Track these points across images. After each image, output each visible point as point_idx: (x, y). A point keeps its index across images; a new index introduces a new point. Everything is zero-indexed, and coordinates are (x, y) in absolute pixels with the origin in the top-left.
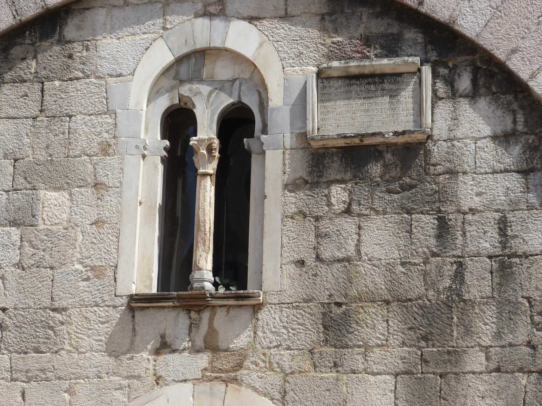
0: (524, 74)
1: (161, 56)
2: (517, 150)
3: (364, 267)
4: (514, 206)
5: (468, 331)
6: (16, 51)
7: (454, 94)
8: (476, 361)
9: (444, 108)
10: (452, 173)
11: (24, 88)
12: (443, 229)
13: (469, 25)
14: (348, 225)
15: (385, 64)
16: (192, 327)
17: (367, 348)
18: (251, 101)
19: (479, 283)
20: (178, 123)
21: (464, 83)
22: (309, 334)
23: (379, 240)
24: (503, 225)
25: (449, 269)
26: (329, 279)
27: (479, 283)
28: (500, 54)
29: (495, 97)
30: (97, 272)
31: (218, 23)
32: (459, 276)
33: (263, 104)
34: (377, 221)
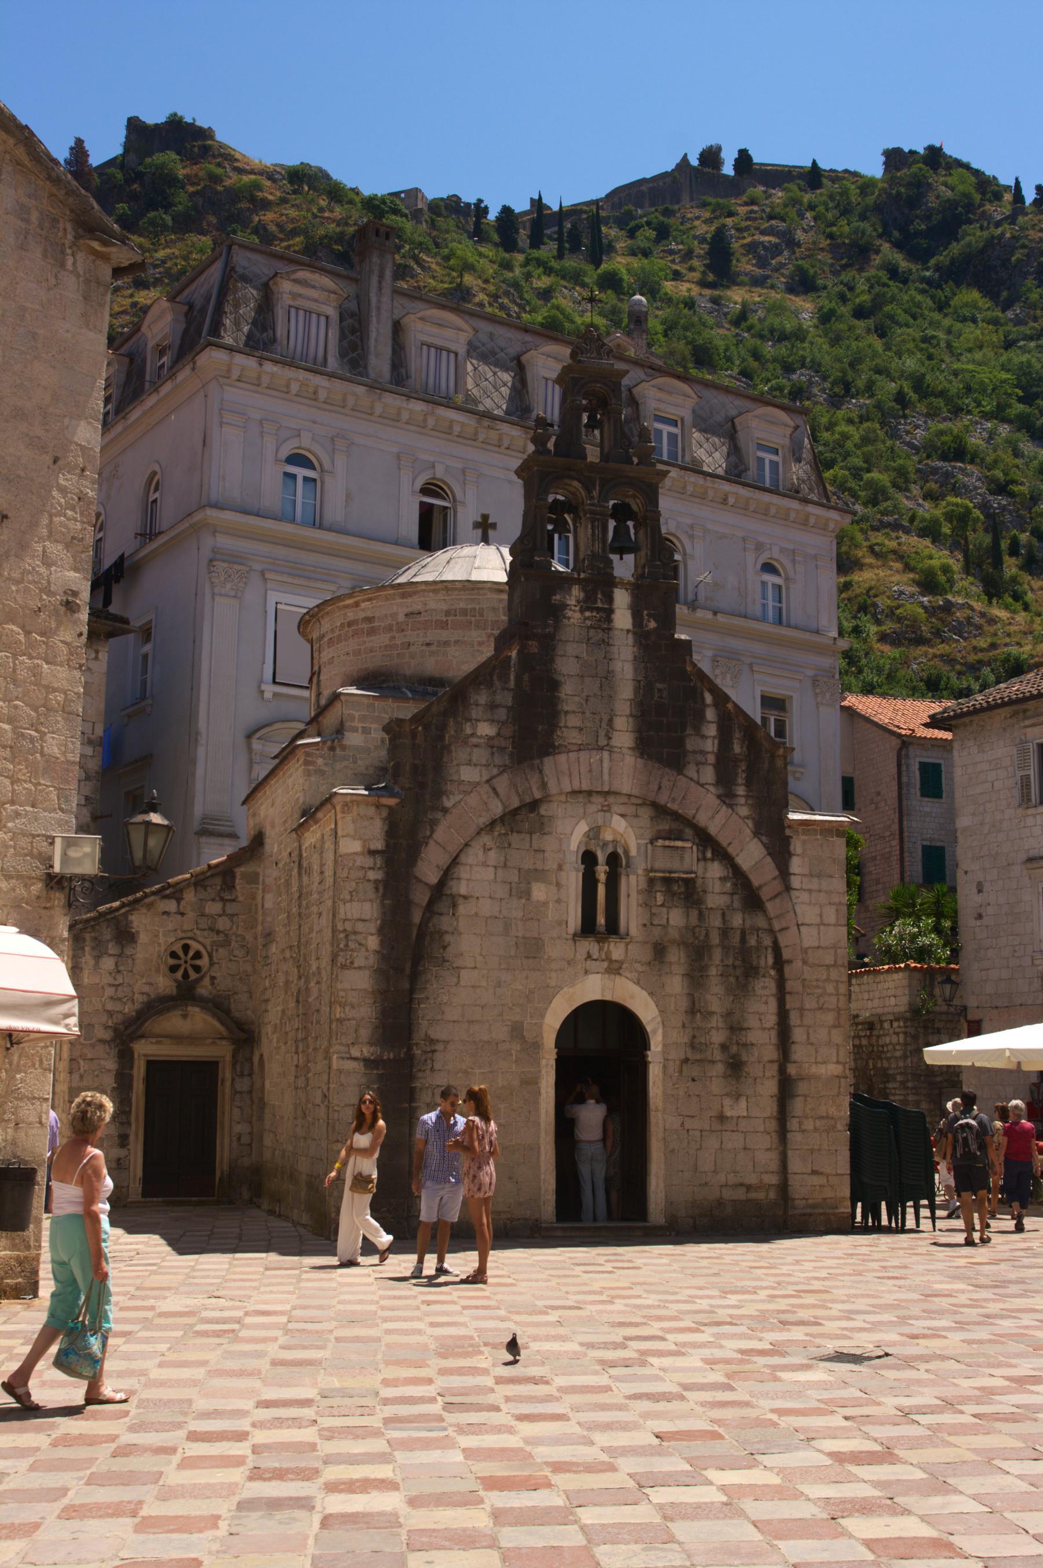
0: (734, 854)
1: (583, 827)
2: (729, 885)
3: (670, 930)
4: (728, 907)
5: (710, 958)
6: (518, 817)
7: (705, 859)
8: (713, 971)
9: (702, 864)
10: (705, 891)
11: (523, 836)
12: (701, 916)
13: (713, 830)
14: (664, 910)
15: (679, 844)
16: (601, 949)
17: (671, 963)
18: (620, 851)
19: (715, 939)
20: (589, 859)
21: (709, 855)
22: (647, 954)
23: (676, 918)
24: (723, 914)
25: (704, 933)
26: (657, 932)
27: (715, 939)
28: (724, 844)
29: (721, 861)
30: (559, 923)
31: (608, 814)
32: (707, 935)
33: (626, 852)
34: (676, 910)
